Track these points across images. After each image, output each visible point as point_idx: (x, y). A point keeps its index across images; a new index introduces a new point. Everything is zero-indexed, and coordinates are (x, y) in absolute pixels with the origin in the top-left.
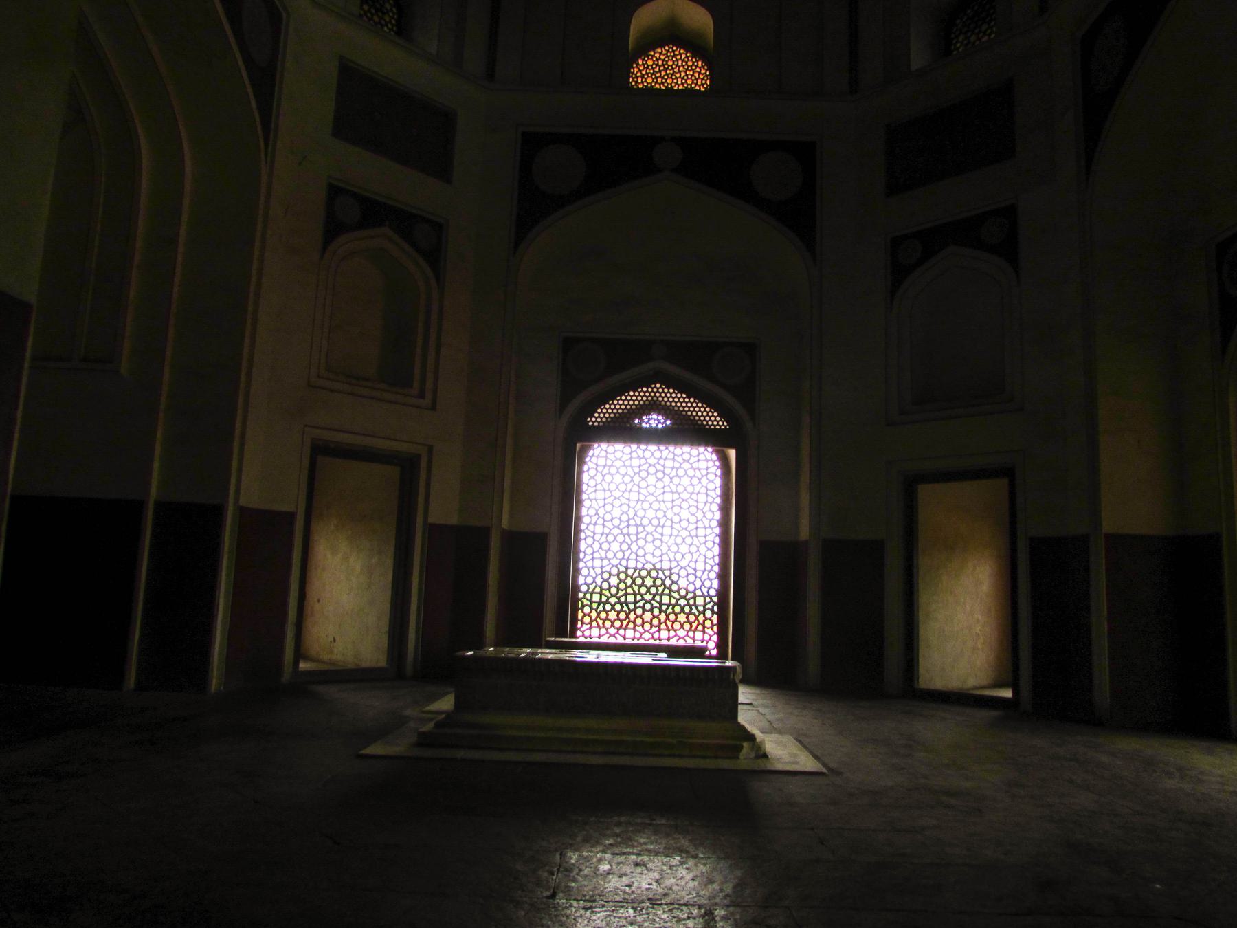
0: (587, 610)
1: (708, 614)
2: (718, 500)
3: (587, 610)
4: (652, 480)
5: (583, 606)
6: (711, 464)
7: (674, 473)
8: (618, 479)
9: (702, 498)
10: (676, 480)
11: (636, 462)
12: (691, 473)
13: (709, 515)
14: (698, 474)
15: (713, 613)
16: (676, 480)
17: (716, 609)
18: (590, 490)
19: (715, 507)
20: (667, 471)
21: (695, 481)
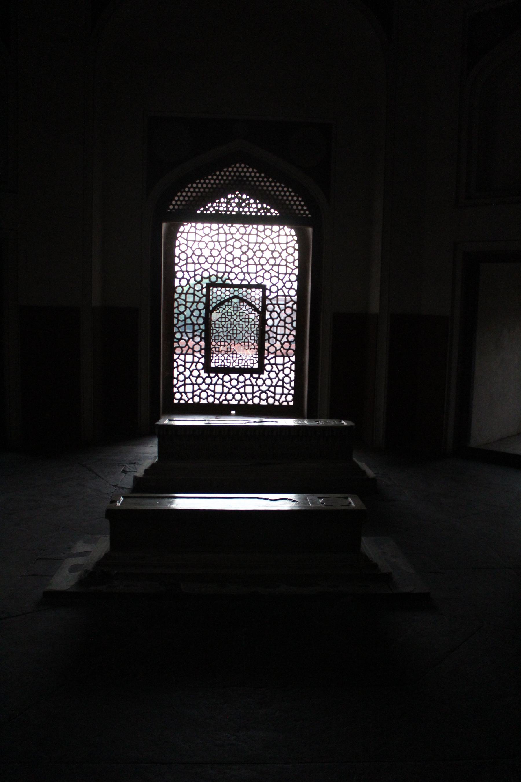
0: (181, 369)
1: (287, 371)
2: (296, 272)
3: (181, 369)
4: (237, 253)
5: (178, 366)
6: (290, 238)
7: (257, 248)
8: (206, 253)
9: (282, 270)
10: (259, 254)
11: (222, 238)
12: (272, 247)
13: (288, 285)
14: (278, 248)
15: (291, 370)
16: (259, 254)
17: (293, 367)
18: (182, 263)
19: (293, 278)
20: (251, 246)
21: (276, 255)
